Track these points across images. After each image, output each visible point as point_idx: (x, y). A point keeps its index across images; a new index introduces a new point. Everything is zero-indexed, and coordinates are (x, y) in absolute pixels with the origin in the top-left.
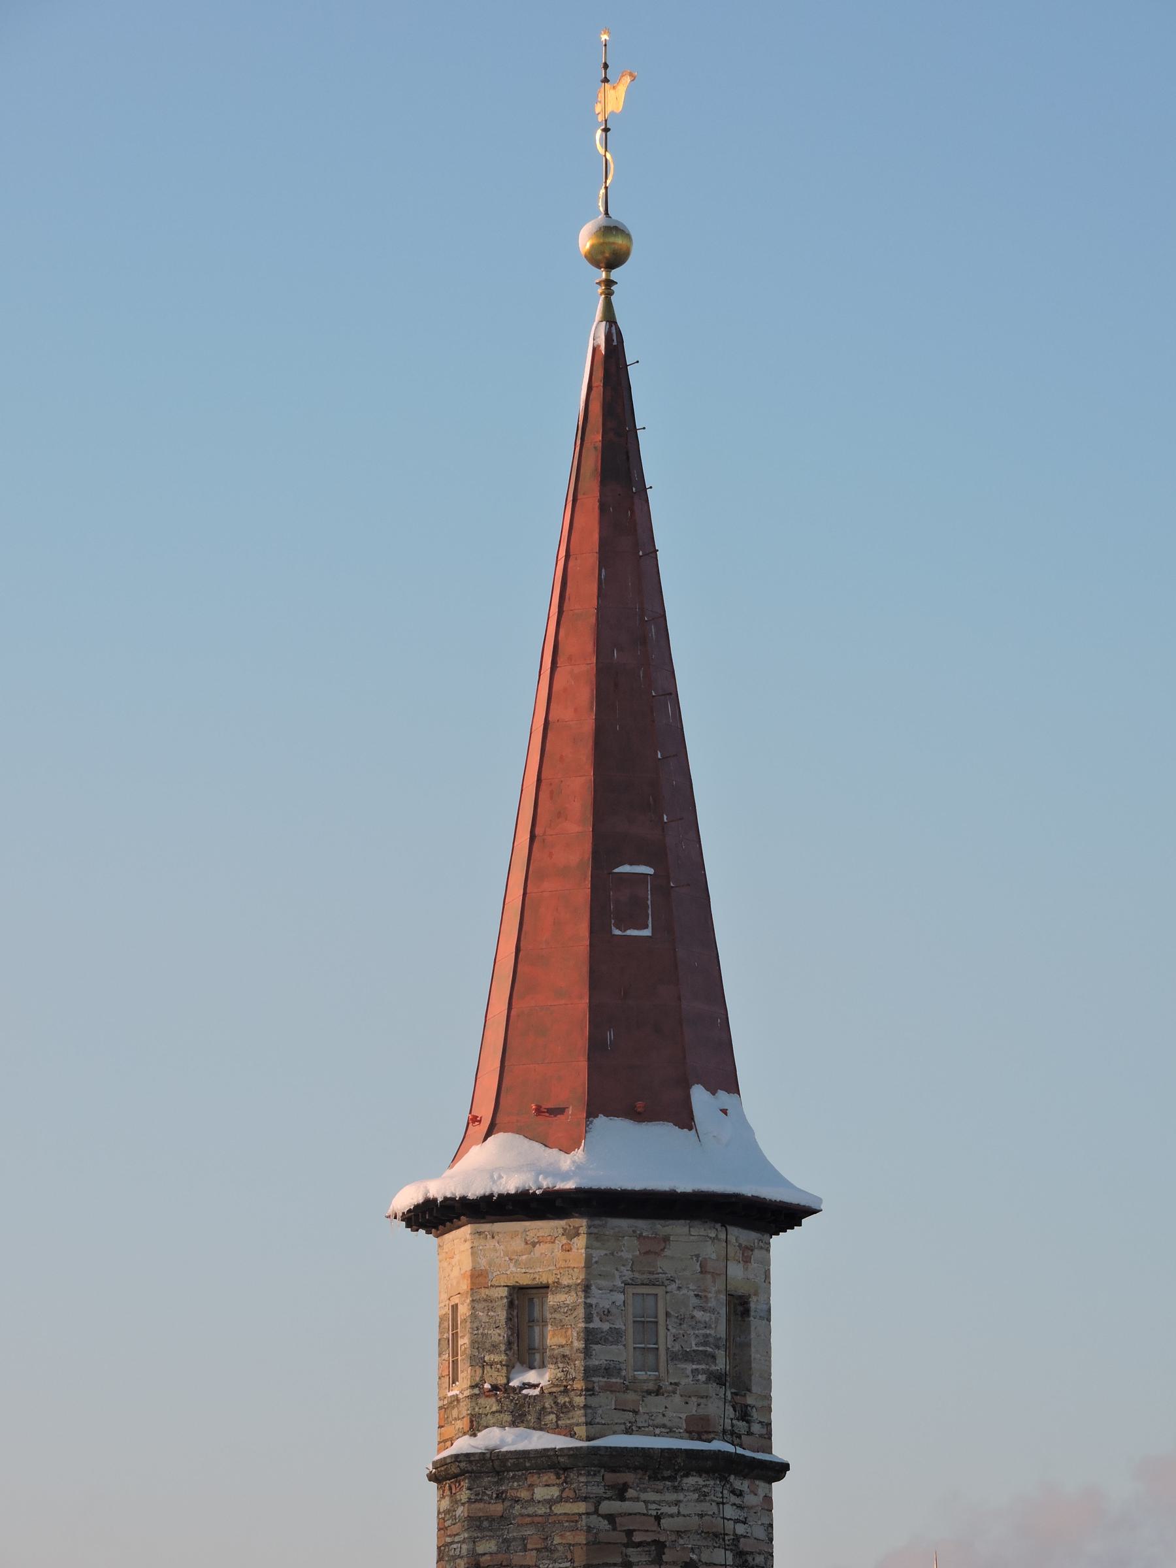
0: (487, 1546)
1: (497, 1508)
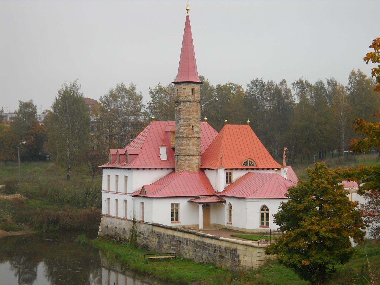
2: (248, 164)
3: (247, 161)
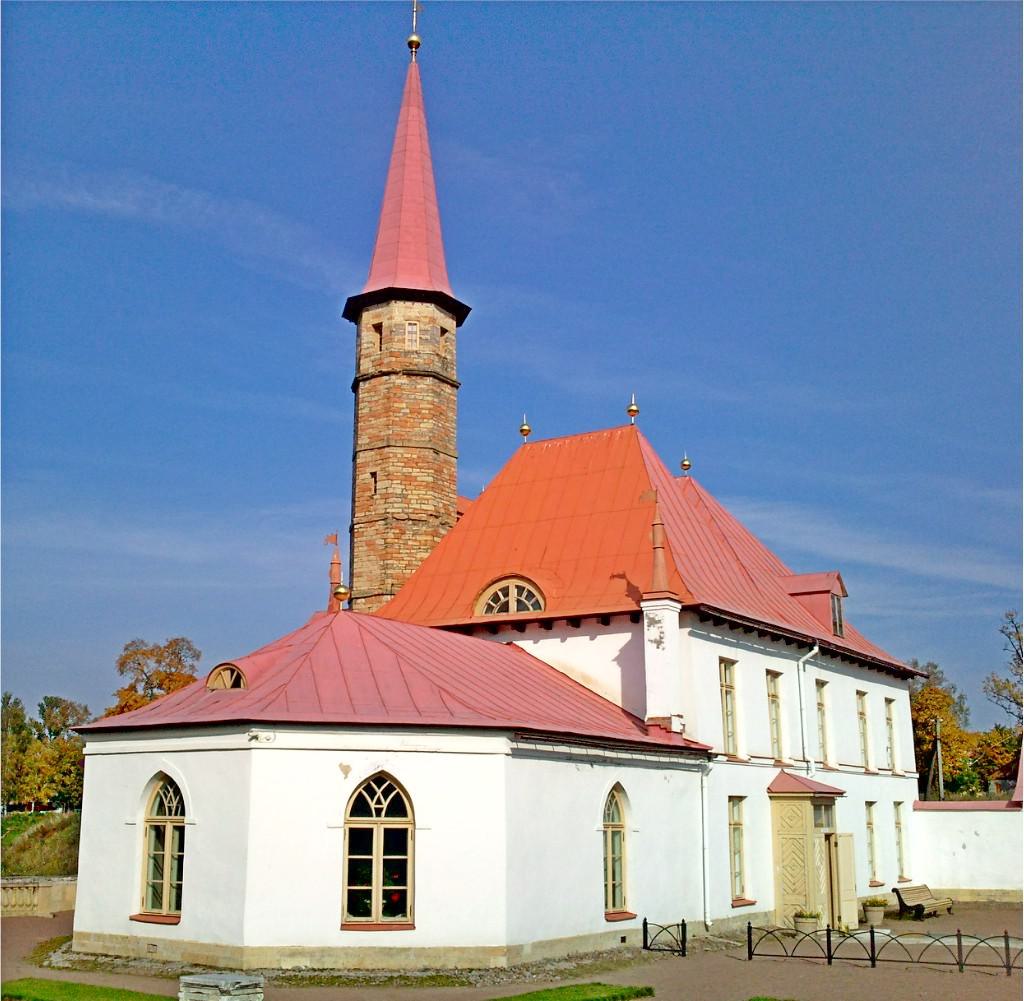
2: (513, 606)
3: (506, 591)
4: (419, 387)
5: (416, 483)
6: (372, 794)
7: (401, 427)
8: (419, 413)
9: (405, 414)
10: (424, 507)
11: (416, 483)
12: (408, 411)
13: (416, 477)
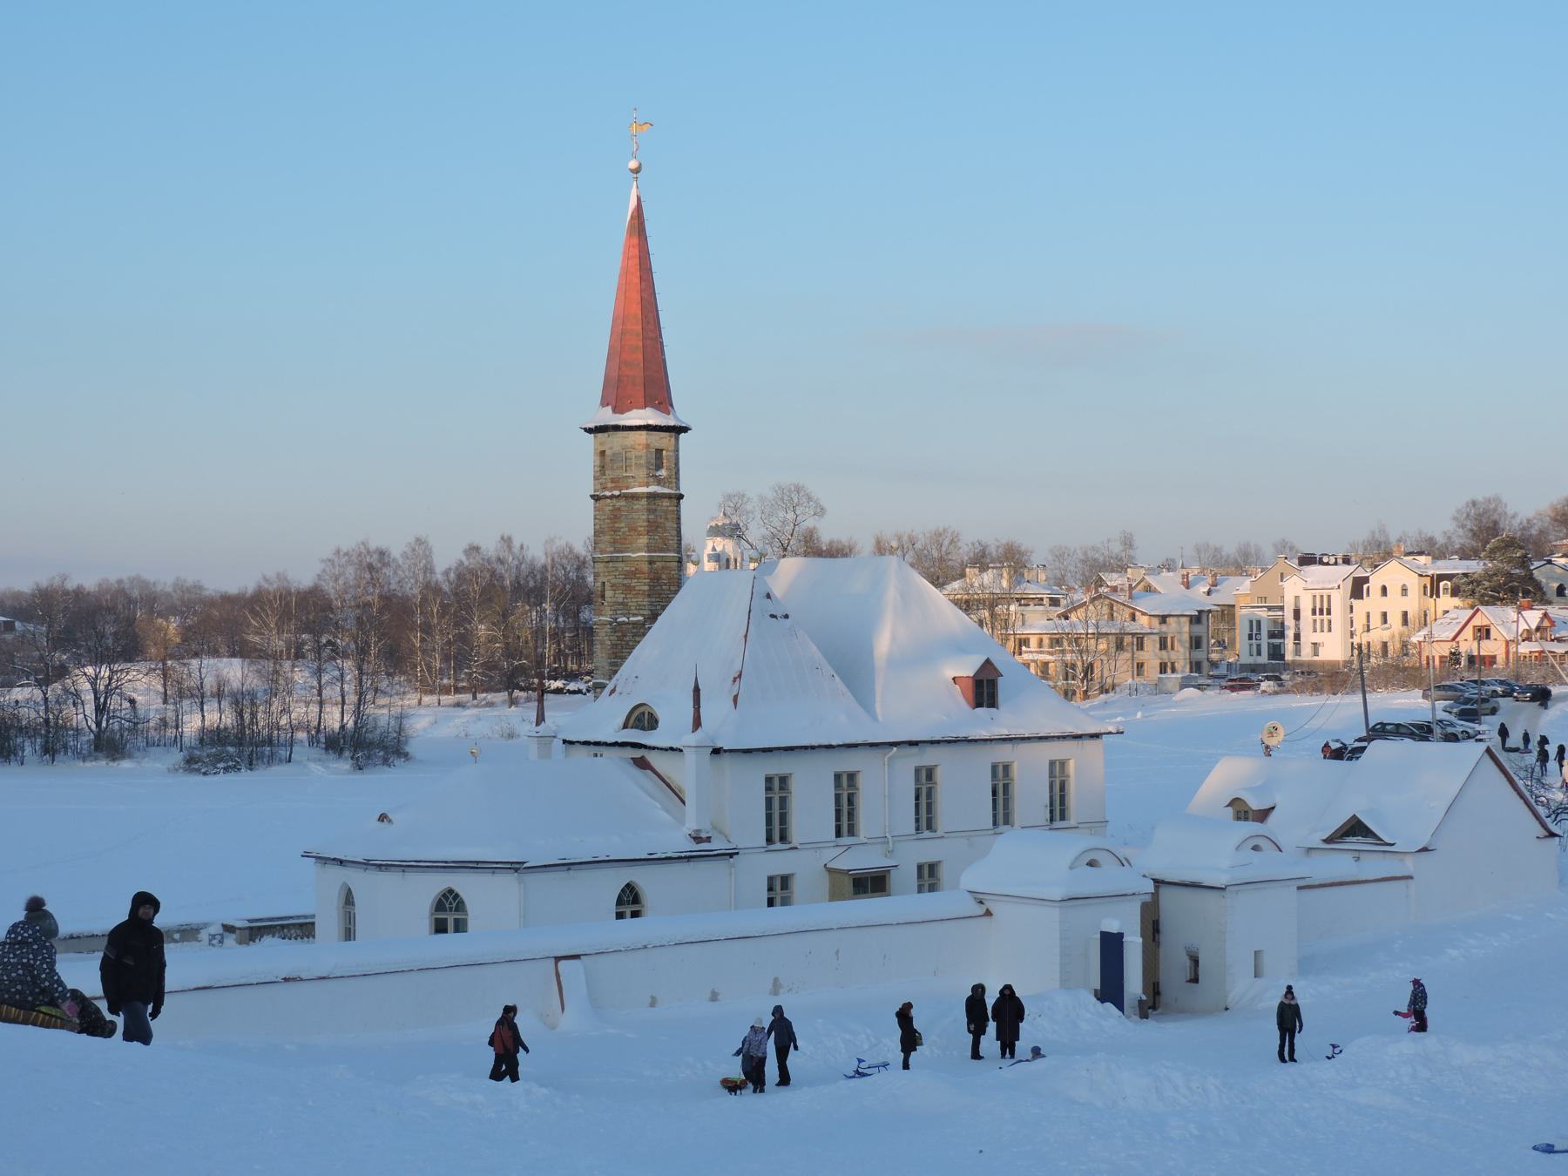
0: (652, 517)
1: (654, 507)
3: (643, 713)
4: (635, 507)
5: (634, 592)
6: (447, 899)
7: (622, 544)
8: (635, 531)
9: (624, 533)
10: (641, 612)
11: (634, 592)
12: (626, 529)
13: (634, 587)
